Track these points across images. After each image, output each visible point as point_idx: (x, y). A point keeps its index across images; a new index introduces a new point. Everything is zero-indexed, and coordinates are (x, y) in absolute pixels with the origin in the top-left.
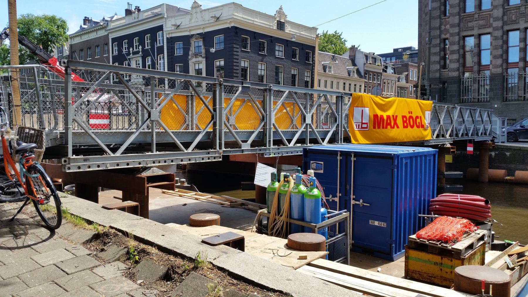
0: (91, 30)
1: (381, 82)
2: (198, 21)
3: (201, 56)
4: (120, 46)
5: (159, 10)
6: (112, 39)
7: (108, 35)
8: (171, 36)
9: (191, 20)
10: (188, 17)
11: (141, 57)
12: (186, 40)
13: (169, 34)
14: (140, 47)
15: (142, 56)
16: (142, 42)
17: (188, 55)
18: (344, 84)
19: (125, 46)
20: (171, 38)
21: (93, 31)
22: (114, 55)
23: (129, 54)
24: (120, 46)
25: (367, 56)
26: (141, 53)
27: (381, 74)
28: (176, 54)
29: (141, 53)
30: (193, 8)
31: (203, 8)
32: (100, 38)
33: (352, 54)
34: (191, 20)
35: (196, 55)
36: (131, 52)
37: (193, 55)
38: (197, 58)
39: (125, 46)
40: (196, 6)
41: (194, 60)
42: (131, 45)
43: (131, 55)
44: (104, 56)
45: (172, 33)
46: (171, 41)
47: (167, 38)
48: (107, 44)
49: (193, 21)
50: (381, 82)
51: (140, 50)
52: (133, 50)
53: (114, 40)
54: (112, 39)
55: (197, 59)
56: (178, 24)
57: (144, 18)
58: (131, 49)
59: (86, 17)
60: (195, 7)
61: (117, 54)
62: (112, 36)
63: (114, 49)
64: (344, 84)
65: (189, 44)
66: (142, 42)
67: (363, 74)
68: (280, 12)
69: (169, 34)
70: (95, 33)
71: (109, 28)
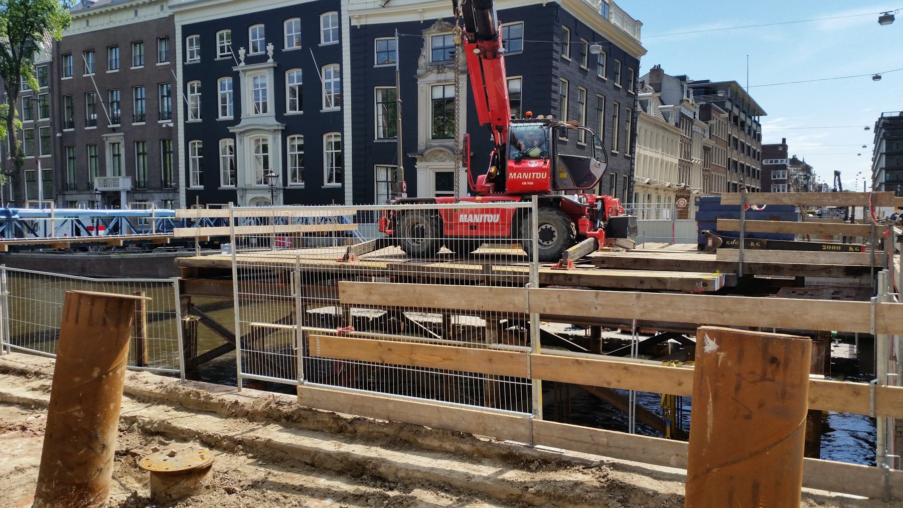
0: (115, 7)
6: (184, 28)
7: (172, 17)
8: (363, 22)
11: (272, 69)
14: (270, 47)
15: (275, 68)
16: (274, 35)
17: (416, 66)
20: (365, 27)
21: (125, 8)
22: (188, 62)
26: (271, 60)
28: (376, 63)
29: (271, 60)
32: (146, 24)
36: (242, 58)
38: (443, 74)
42: (240, 40)
43: (243, 64)
44: (157, 65)
45: (367, 16)
47: (353, 29)
48: (168, 38)
51: (270, 53)
52: (247, 52)
53: (188, 30)
54: (184, 28)
58: (242, 52)
61: (199, 62)
62: (179, 22)
63: (188, 49)
65: (420, 43)
66: (274, 35)
70: (131, 14)
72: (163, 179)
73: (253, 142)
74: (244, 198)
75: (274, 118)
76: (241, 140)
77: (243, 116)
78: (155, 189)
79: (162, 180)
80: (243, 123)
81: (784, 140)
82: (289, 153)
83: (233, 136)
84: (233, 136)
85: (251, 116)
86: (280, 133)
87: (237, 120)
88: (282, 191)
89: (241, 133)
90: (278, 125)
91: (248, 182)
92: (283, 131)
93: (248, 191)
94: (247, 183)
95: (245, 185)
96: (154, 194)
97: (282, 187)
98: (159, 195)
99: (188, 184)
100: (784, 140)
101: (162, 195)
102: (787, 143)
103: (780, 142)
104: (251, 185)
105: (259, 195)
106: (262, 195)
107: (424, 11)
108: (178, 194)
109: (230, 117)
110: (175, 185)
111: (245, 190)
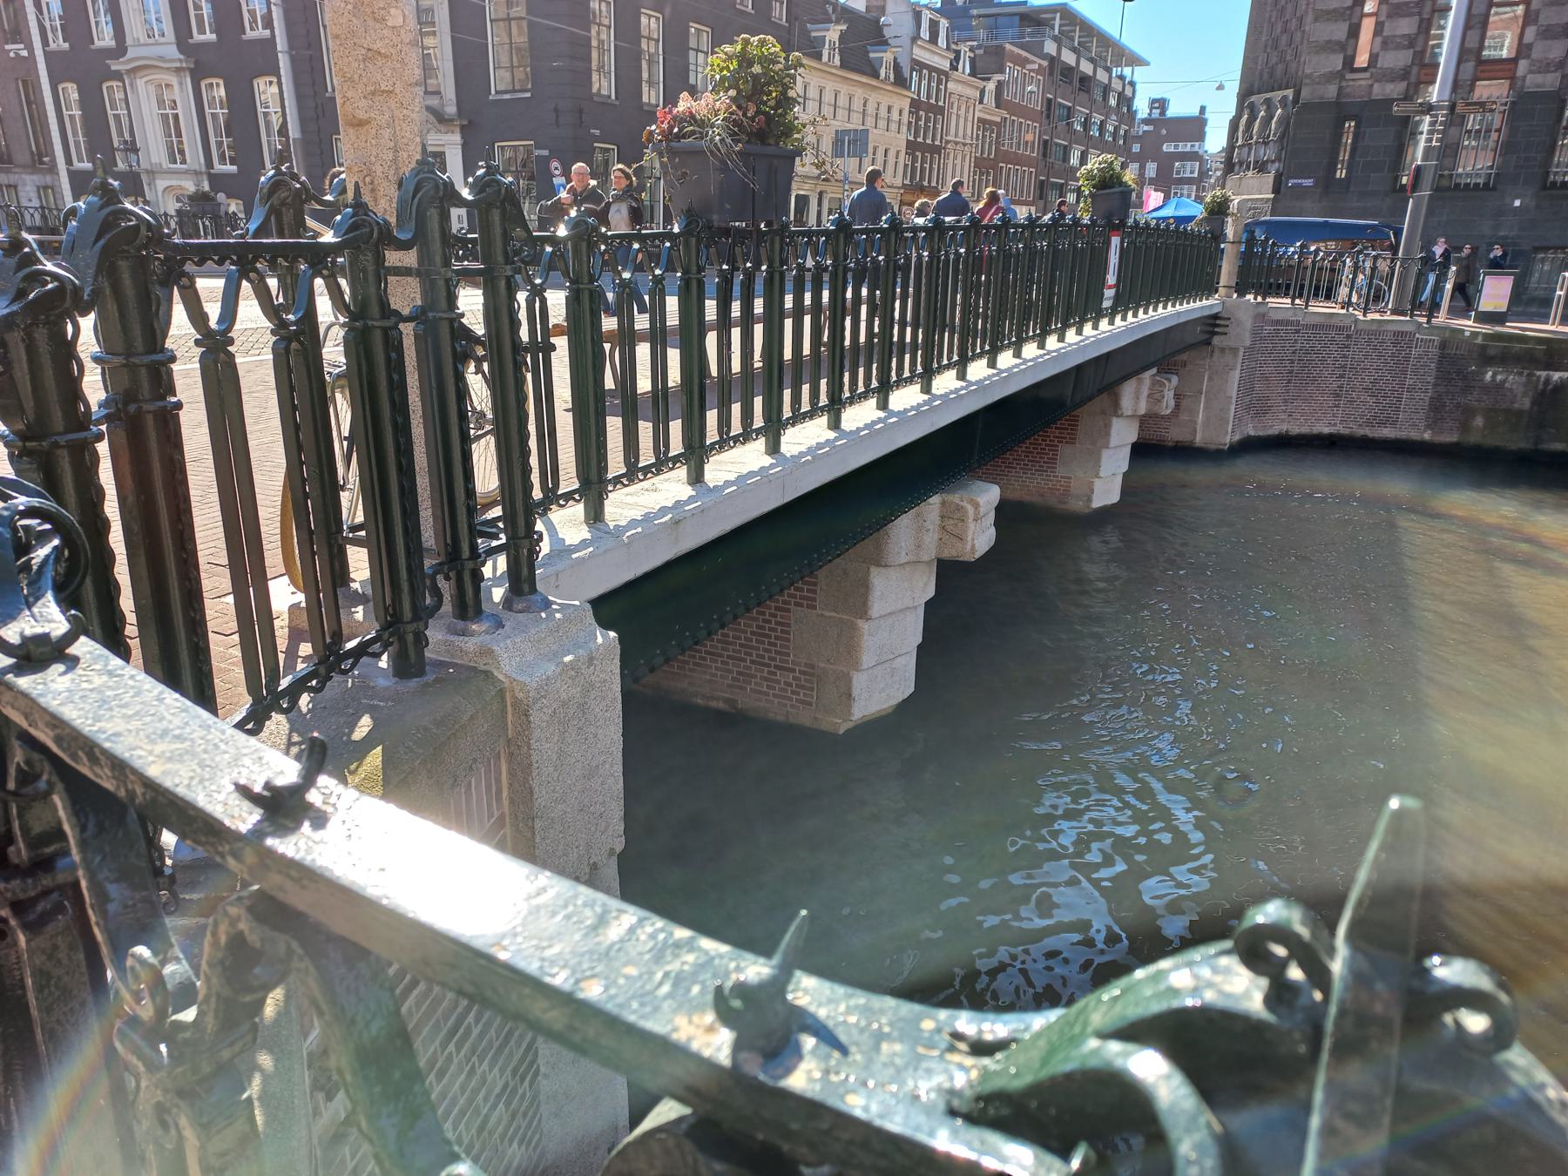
72: (34, 149)
73: (152, 89)
74: (153, 187)
75: (175, 46)
76: (131, 85)
77: (129, 41)
78: (24, 167)
79: (32, 152)
80: (131, 53)
81: (1203, 109)
82: (207, 110)
83: (118, 76)
84: (118, 76)
85: (142, 41)
86: (188, 74)
87: (120, 49)
88: (205, 177)
89: (129, 72)
90: (180, 61)
91: (155, 160)
93: (157, 176)
94: (153, 161)
95: (151, 164)
96: (24, 176)
97: (203, 169)
98: (32, 177)
99: (69, 161)
100: (1203, 109)
101: (35, 177)
102: (1207, 115)
103: (1195, 112)
104: (160, 164)
105: (174, 183)
106: (179, 183)
108: (56, 177)
110: (50, 161)
111: (151, 173)
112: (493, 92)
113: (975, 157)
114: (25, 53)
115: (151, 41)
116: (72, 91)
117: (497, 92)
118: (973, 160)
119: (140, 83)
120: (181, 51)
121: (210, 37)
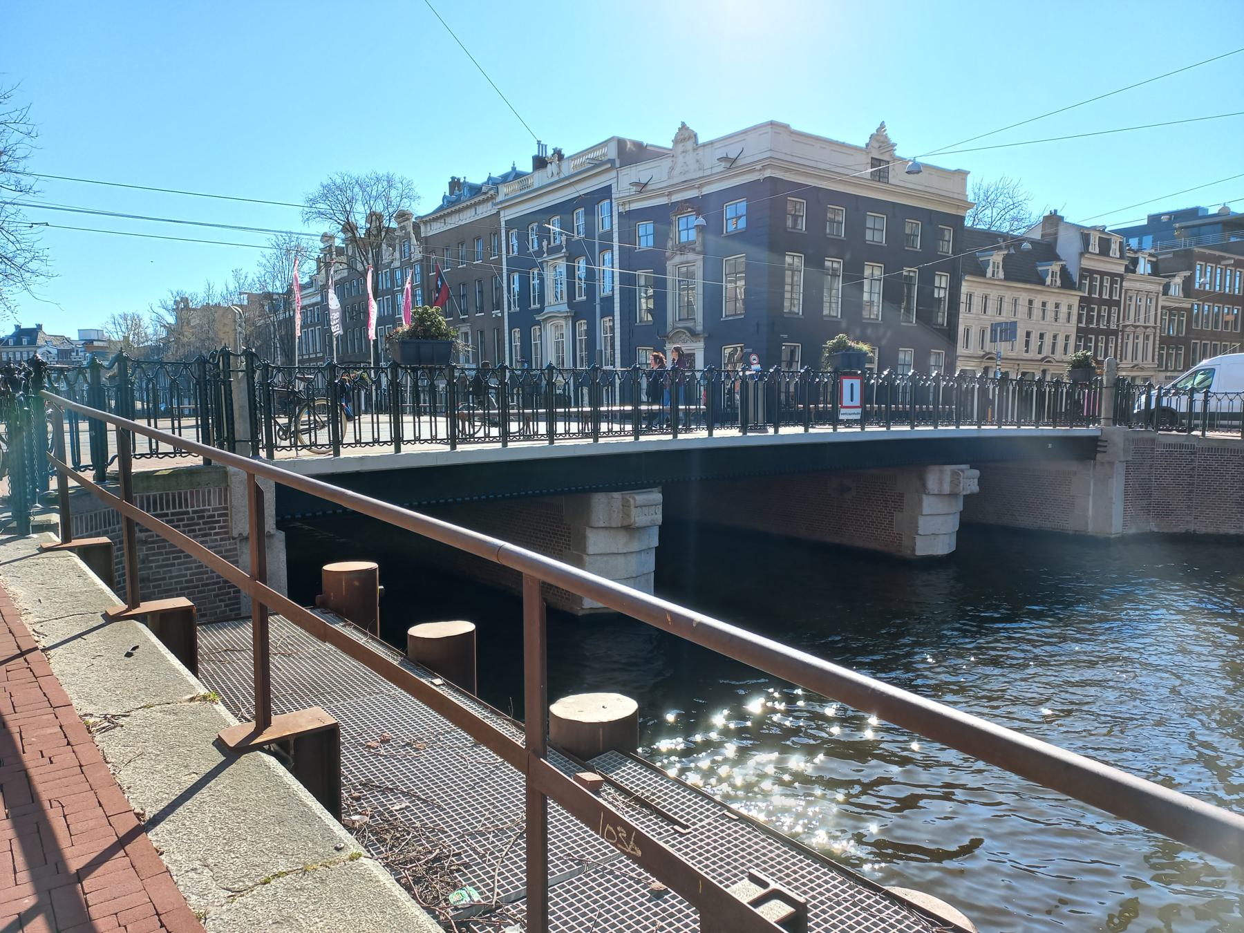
1: (1120, 297)
2: (687, 171)
3: (694, 250)
4: (523, 240)
5: (604, 150)
9: (672, 169)
10: (666, 164)
12: (662, 216)
13: (624, 204)
18: (1031, 302)
19: (533, 237)
23: (540, 253)
24: (523, 240)
25: (1084, 235)
26: (564, 250)
27: (1121, 276)
29: (564, 250)
30: (676, 141)
31: (701, 140)
33: (1048, 231)
34: (672, 169)
35: (683, 248)
37: (675, 249)
39: (533, 237)
40: (685, 135)
41: (678, 259)
43: (545, 255)
45: (629, 202)
46: (630, 218)
47: (620, 214)
49: (676, 172)
50: (1120, 297)
52: (549, 243)
55: (684, 258)
56: (644, 181)
57: (572, 171)
58: (545, 243)
59: (453, 178)
60: (683, 140)
64: (1031, 302)
67: (1076, 279)
68: (880, 139)
69: (624, 204)
71: (500, 198)
77: (546, 304)
83: (538, 323)
84: (538, 323)
87: (542, 309)
89: (543, 320)
92: (572, 317)
107: (670, 194)
109: (538, 306)
112: (724, 316)
113: (1160, 337)
114: (500, 315)
115: (557, 303)
116: (517, 333)
117: (726, 316)
118: (1158, 338)
119: (548, 326)
120: (569, 307)
121: (584, 298)
